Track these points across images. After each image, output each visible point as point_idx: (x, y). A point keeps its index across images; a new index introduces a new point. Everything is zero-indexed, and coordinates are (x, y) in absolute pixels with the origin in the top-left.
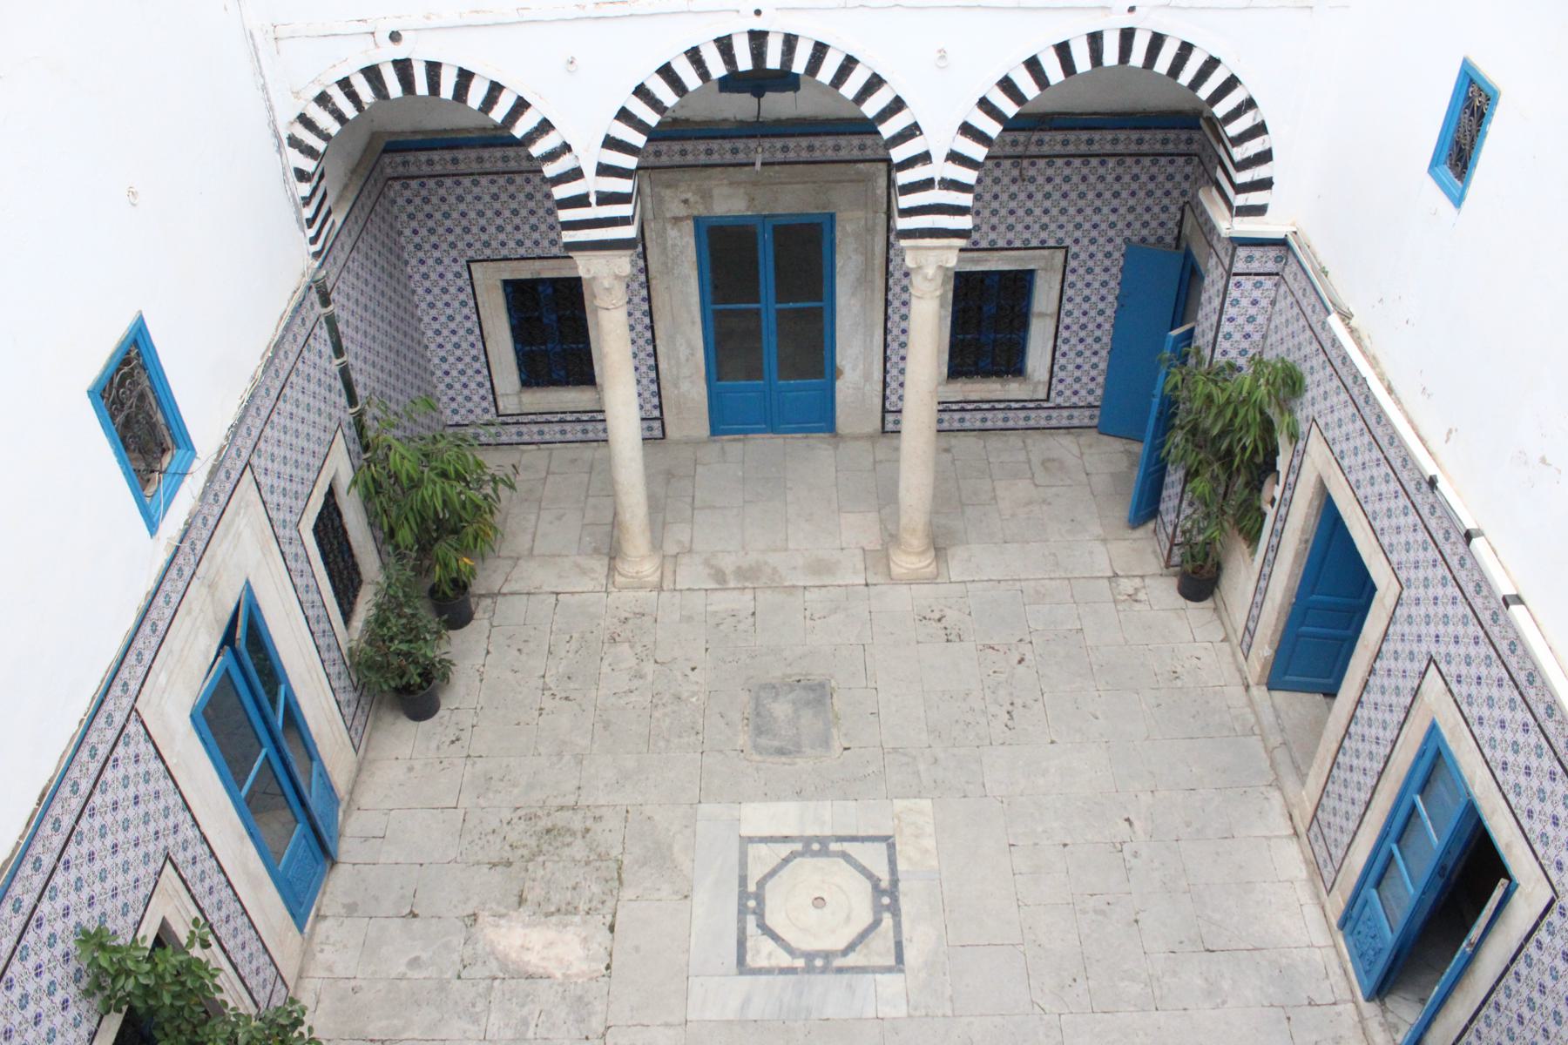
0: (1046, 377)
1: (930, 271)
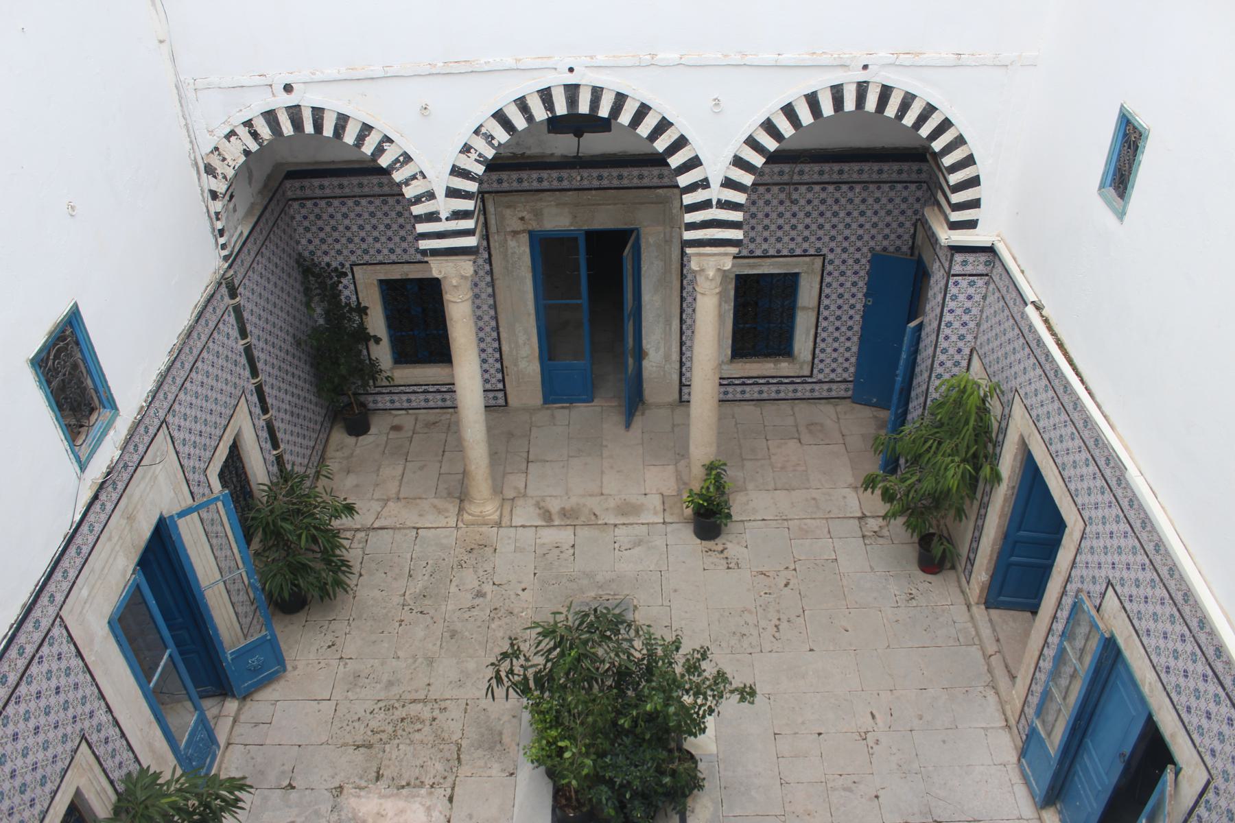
0: (810, 357)
1: (711, 273)
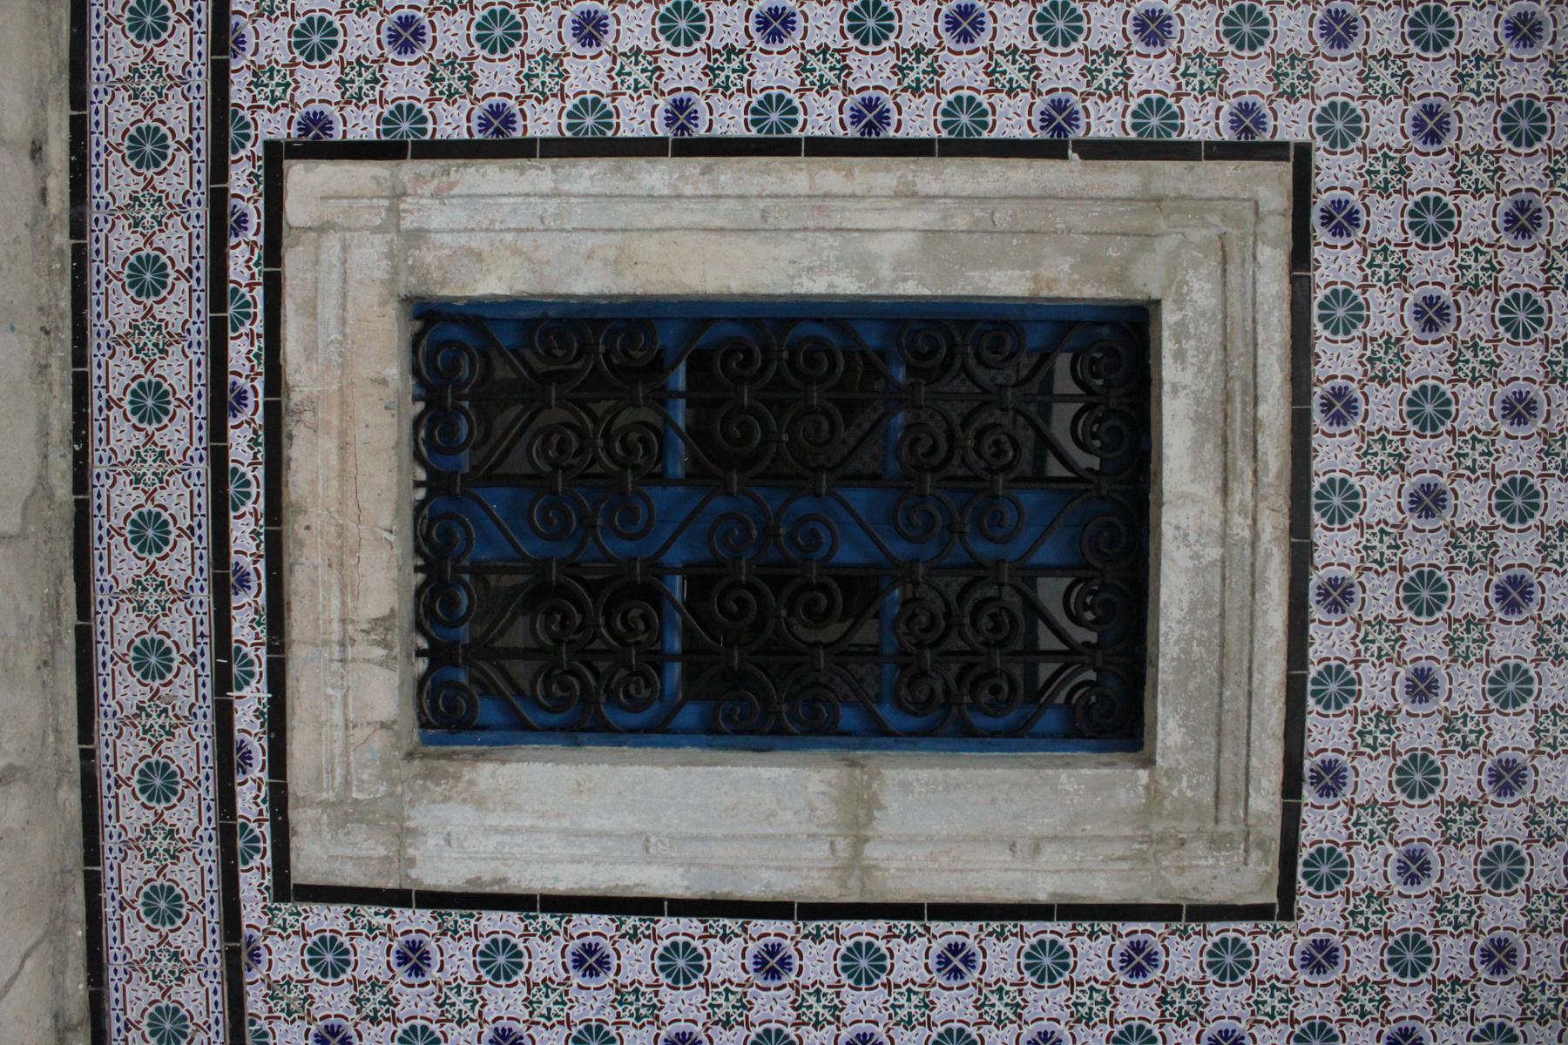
0: (442, 870)
